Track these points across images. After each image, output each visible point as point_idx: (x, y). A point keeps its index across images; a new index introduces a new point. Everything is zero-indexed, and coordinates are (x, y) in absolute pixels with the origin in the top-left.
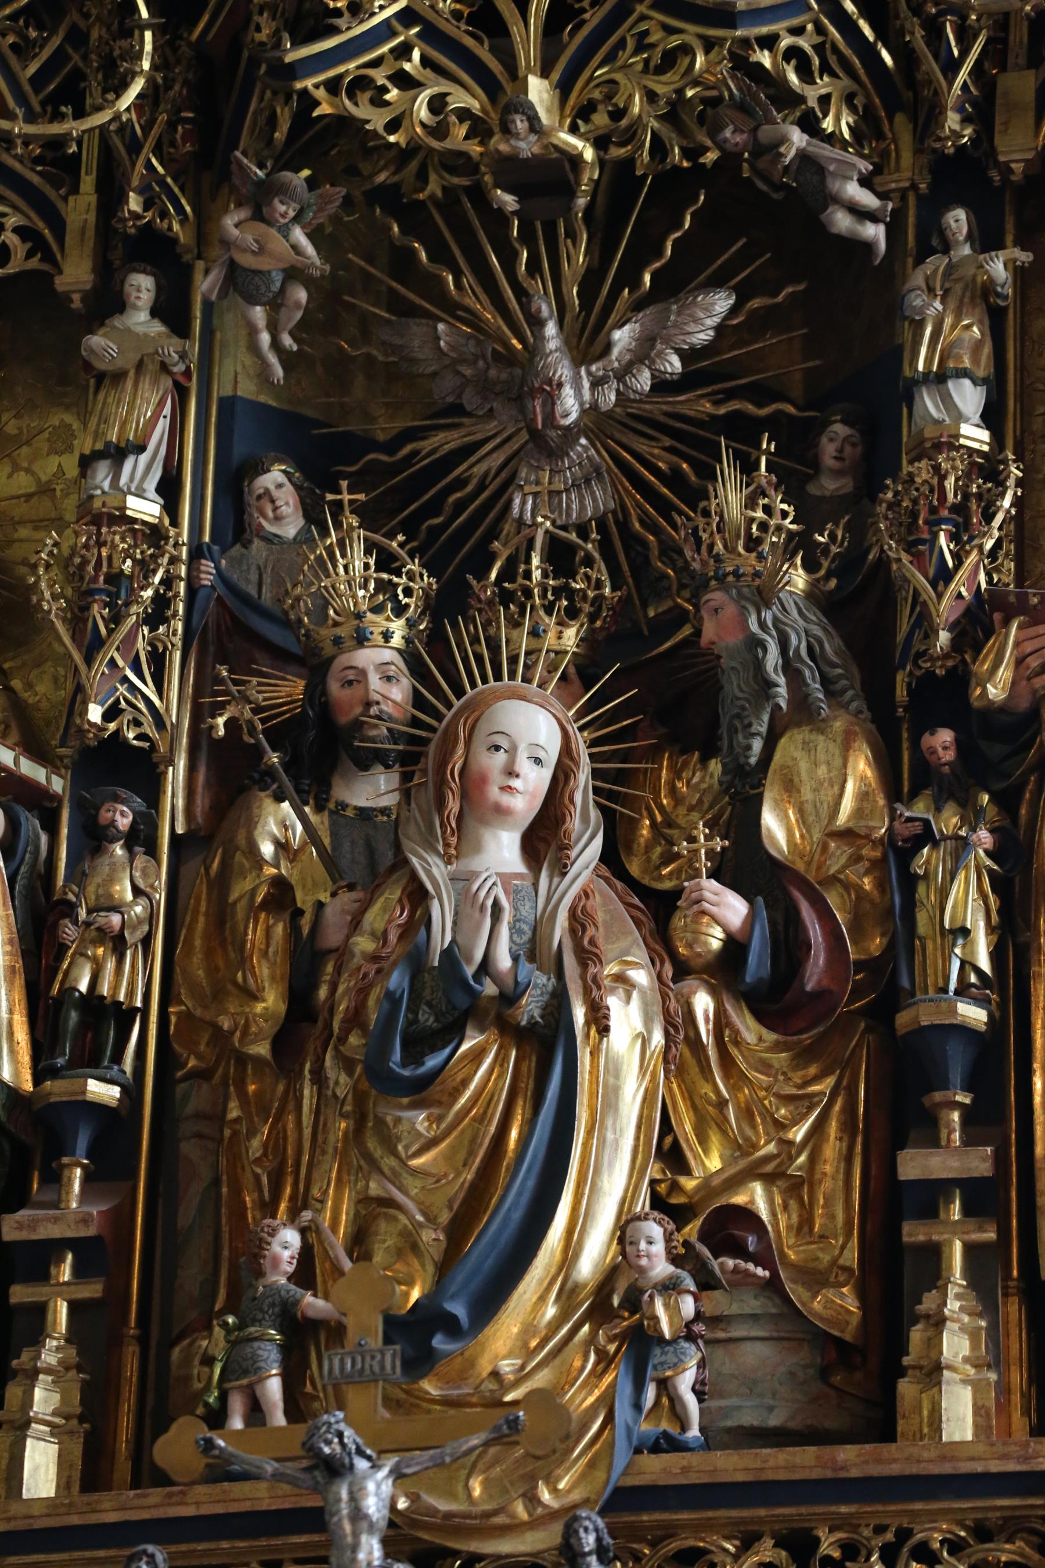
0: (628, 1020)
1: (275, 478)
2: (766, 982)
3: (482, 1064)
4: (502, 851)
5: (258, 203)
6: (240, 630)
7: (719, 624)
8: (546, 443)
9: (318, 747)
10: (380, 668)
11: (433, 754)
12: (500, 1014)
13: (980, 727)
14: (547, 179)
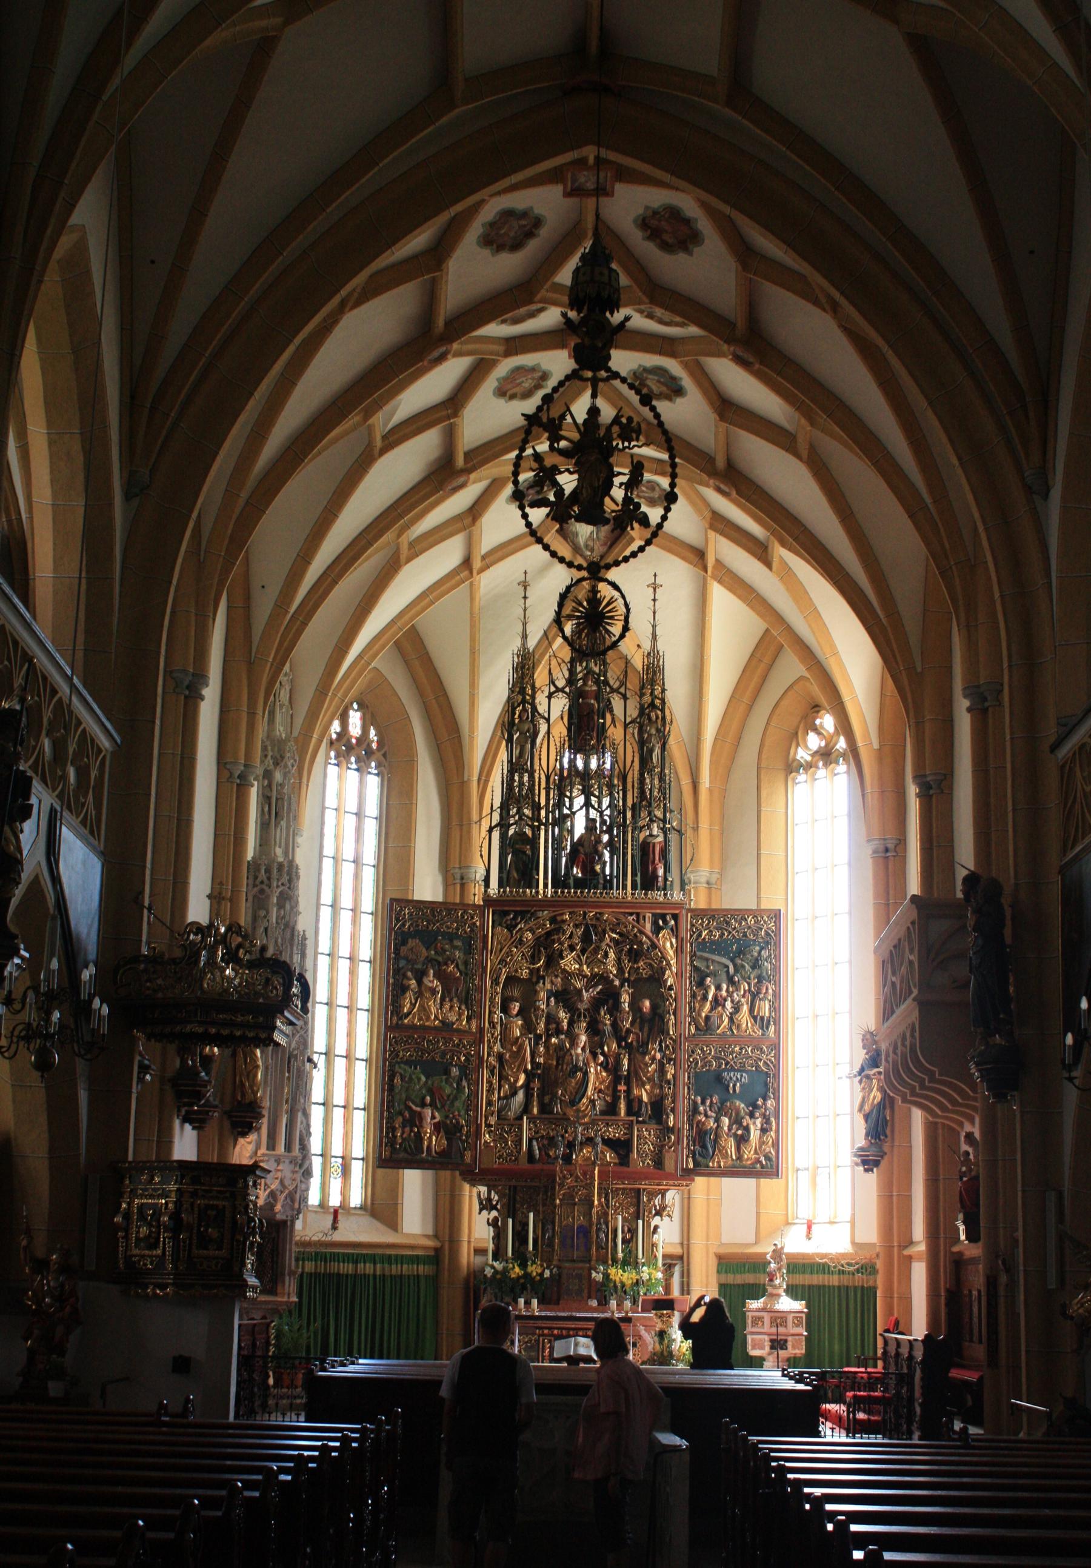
0: (592, 1070)
1: (552, 999)
2: (605, 1066)
4: (579, 1051)
5: (556, 976)
6: (551, 1019)
7: (600, 1026)
8: (582, 1001)
9: (558, 1032)
12: (581, 1069)
13: (627, 1043)
14: (585, 976)
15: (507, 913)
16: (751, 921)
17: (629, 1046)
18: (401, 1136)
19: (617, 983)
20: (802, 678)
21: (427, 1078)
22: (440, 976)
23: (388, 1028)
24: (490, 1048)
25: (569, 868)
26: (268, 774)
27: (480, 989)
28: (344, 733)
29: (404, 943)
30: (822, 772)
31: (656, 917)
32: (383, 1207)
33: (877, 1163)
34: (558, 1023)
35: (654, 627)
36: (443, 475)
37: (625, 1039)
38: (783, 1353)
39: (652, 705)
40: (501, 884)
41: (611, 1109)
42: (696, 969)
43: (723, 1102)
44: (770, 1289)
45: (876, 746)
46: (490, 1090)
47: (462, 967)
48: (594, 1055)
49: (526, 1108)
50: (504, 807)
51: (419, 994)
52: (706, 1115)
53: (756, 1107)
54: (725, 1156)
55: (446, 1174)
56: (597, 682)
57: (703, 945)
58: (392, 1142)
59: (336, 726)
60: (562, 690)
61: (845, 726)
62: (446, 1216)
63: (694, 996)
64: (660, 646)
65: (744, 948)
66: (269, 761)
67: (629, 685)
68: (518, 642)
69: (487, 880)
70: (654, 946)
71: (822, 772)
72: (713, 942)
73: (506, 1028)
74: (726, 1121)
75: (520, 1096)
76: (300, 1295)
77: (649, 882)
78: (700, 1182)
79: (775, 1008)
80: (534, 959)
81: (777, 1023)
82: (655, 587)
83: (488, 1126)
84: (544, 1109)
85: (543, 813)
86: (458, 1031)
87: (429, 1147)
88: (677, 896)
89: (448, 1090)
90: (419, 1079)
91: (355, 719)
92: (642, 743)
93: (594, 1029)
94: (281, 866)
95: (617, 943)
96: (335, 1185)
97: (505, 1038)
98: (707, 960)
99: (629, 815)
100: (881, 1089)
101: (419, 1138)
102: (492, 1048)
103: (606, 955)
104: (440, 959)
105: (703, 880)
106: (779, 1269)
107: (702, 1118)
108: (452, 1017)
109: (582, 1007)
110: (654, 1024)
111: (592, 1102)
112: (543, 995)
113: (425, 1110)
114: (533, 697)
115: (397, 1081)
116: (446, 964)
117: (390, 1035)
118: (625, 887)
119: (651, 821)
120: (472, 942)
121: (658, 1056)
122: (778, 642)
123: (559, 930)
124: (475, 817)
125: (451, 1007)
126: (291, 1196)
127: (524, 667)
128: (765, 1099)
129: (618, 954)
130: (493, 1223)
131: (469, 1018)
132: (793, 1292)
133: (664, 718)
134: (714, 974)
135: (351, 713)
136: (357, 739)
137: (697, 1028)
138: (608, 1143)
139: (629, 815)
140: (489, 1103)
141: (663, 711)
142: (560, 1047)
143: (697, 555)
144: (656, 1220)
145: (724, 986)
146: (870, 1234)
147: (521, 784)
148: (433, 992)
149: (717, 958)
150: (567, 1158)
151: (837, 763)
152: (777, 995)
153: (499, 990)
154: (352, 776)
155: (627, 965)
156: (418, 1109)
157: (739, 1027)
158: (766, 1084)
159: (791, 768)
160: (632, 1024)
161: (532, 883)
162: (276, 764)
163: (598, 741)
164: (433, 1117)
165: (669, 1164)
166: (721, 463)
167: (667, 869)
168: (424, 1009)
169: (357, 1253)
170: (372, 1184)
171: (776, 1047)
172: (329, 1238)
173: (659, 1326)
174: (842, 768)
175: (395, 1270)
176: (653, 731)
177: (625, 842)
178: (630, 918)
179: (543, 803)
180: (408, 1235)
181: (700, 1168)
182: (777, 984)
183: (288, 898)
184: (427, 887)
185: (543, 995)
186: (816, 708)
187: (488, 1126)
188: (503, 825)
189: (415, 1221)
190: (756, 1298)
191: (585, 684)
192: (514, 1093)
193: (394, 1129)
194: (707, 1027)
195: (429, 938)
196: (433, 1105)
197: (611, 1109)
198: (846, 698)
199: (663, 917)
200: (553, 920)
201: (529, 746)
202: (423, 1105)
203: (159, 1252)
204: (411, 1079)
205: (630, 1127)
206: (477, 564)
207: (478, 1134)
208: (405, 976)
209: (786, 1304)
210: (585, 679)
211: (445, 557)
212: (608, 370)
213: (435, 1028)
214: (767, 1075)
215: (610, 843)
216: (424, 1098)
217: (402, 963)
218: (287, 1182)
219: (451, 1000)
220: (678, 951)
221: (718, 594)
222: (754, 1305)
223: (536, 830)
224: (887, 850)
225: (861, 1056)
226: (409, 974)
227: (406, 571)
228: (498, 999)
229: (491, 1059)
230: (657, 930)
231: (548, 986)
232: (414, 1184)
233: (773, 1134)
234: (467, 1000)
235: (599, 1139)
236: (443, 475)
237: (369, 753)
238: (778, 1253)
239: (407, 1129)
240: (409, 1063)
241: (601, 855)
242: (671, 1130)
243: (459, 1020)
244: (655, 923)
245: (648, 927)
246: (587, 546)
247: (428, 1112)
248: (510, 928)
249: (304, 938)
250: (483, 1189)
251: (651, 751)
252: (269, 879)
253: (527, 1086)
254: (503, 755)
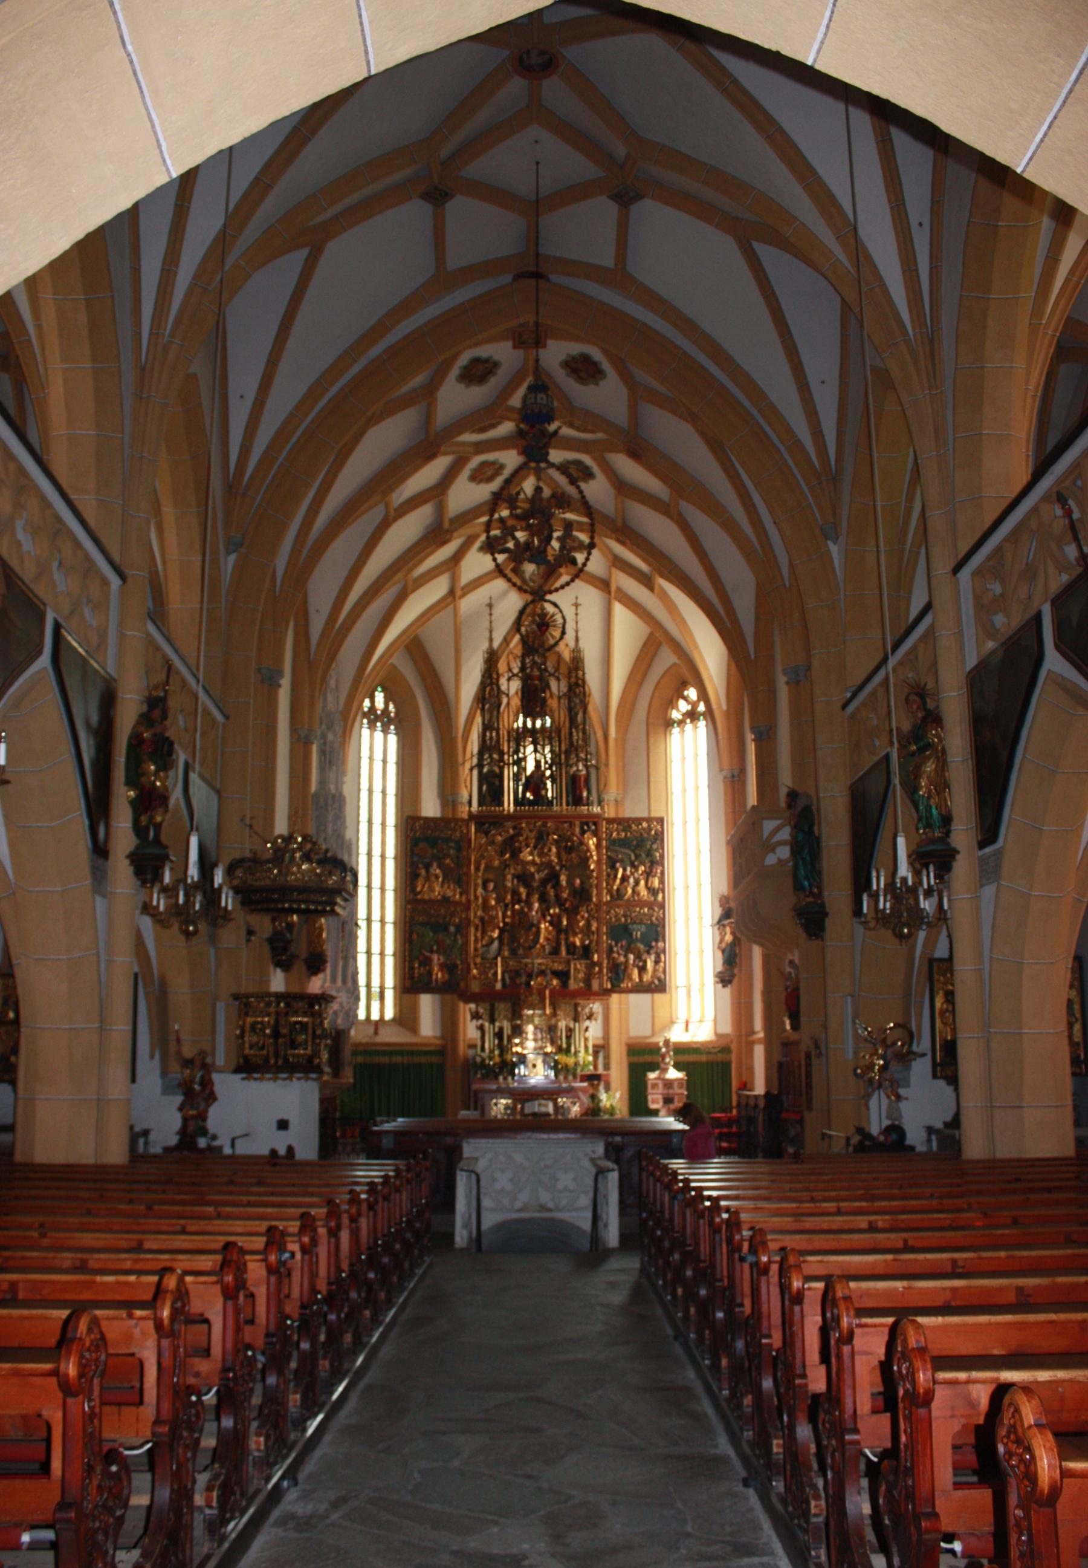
2: (551, 923)
3: (534, 929)
4: (534, 913)
6: (515, 893)
9: (519, 901)
10: (524, 896)
11: (530, 907)
15: (484, 824)
16: (645, 825)
17: (566, 910)
19: (558, 868)
20: (675, 664)
22: (439, 867)
23: (408, 902)
24: (475, 914)
25: (524, 793)
26: (324, 736)
27: (468, 874)
28: (372, 708)
30: (689, 726)
31: (582, 824)
32: (406, 1018)
33: (730, 982)
34: (519, 895)
35: (577, 632)
36: (436, 535)
37: (564, 905)
38: (672, 1106)
39: (577, 685)
40: (480, 804)
41: (555, 951)
42: (609, 857)
43: (629, 945)
44: (662, 1066)
45: (724, 707)
46: (476, 940)
48: (544, 916)
49: (499, 952)
50: (481, 754)
51: (427, 879)
52: (618, 953)
53: (651, 947)
54: (631, 979)
55: (448, 997)
56: (540, 669)
57: (612, 842)
58: (412, 978)
59: (367, 703)
60: (516, 675)
61: (703, 695)
62: (449, 1023)
63: (608, 875)
64: (581, 644)
65: (642, 844)
66: (324, 727)
67: (561, 671)
68: (486, 645)
69: (470, 803)
70: (581, 843)
71: (689, 726)
72: (620, 840)
73: (486, 901)
74: (631, 957)
75: (496, 944)
76: (355, 1077)
77: (577, 801)
78: (615, 997)
79: (662, 881)
80: (502, 854)
81: (663, 892)
82: (577, 605)
83: (475, 964)
84: (514, 952)
85: (506, 757)
88: (596, 810)
89: (448, 941)
91: (380, 698)
92: (570, 709)
93: (543, 899)
94: (334, 796)
95: (556, 842)
96: (375, 1005)
97: (486, 906)
98: (616, 851)
99: (563, 757)
100: (733, 933)
101: (430, 973)
102: (476, 913)
103: (550, 850)
105: (612, 799)
106: (668, 1052)
107: (615, 955)
108: (449, 893)
109: (535, 884)
110: (582, 895)
111: (543, 947)
112: (509, 877)
114: (498, 680)
115: (415, 936)
117: (409, 907)
118: (561, 805)
119: (578, 761)
120: (463, 843)
121: (586, 915)
122: (658, 640)
123: (519, 834)
124: (460, 760)
125: (449, 887)
126: (347, 1014)
127: (491, 660)
128: (657, 941)
129: (558, 848)
130: (481, 1028)
131: (461, 894)
132: (678, 1066)
133: (585, 692)
134: (621, 861)
135: (377, 693)
137: (612, 897)
138: (556, 974)
139: (563, 757)
140: (476, 949)
141: (584, 687)
142: (521, 911)
143: (604, 585)
144: (587, 1023)
145: (629, 869)
146: (727, 1028)
147: (491, 738)
148: (437, 877)
149: (623, 850)
150: (528, 984)
151: (698, 719)
152: (662, 873)
153: (480, 874)
154: (379, 735)
155: (564, 856)
157: (638, 894)
158: (657, 933)
159: (669, 724)
160: (569, 894)
161: (501, 803)
162: (329, 728)
163: (542, 708)
165: (595, 985)
166: (619, 523)
167: (589, 792)
168: (431, 889)
169: (391, 1050)
170: (399, 1004)
171: (662, 906)
172: (372, 1041)
173: (591, 1091)
174: (702, 724)
175: (416, 1060)
176: (578, 701)
177: (561, 775)
178: (566, 825)
179: (506, 750)
180: (426, 1037)
181: (616, 988)
182: (663, 866)
183: (340, 817)
184: (430, 807)
185: (509, 877)
186: (684, 685)
187: (475, 964)
188: (480, 766)
189: (428, 1026)
190: (653, 1070)
191: (532, 670)
192: (492, 940)
193: (412, 968)
194: (619, 895)
195: (433, 842)
196: (438, 952)
197: (555, 951)
198: (705, 676)
199: (587, 824)
200: (514, 828)
201: (495, 713)
202: (432, 951)
203: (265, 1052)
205: (568, 963)
206: (458, 592)
207: (469, 970)
208: (417, 867)
209: (673, 1074)
210: (532, 667)
211: (437, 589)
212: (547, 462)
213: (438, 901)
214: (658, 926)
215: (551, 776)
216: (432, 947)
218: (345, 1005)
220: (598, 846)
221: (619, 609)
222: (652, 1076)
223: (502, 769)
224: (733, 776)
225: (719, 911)
226: (420, 866)
227: (412, 598)
228: (480, 881)
229: (477, 921)
230: (583, 832)
231: (512, 871)
232: (427, 1003)
233: (662, 964)
234: (459, 882)
235: (548, 971)
236: (436, 535)
237: (390, 721)
238: (667, 1042)
240: (422, 924)
241: (545, 784)
242: (594, 964)
243: (454, 895)
244: (582, 829)
245: (577, 830)
246: (531, 580)
247: (435, 957)
248: (486, 833)
249: (350, 844)
250: (473, 1006)
251: (577, 714)
252: (326, 805)
253: (500, 937)
254: (478, 720)
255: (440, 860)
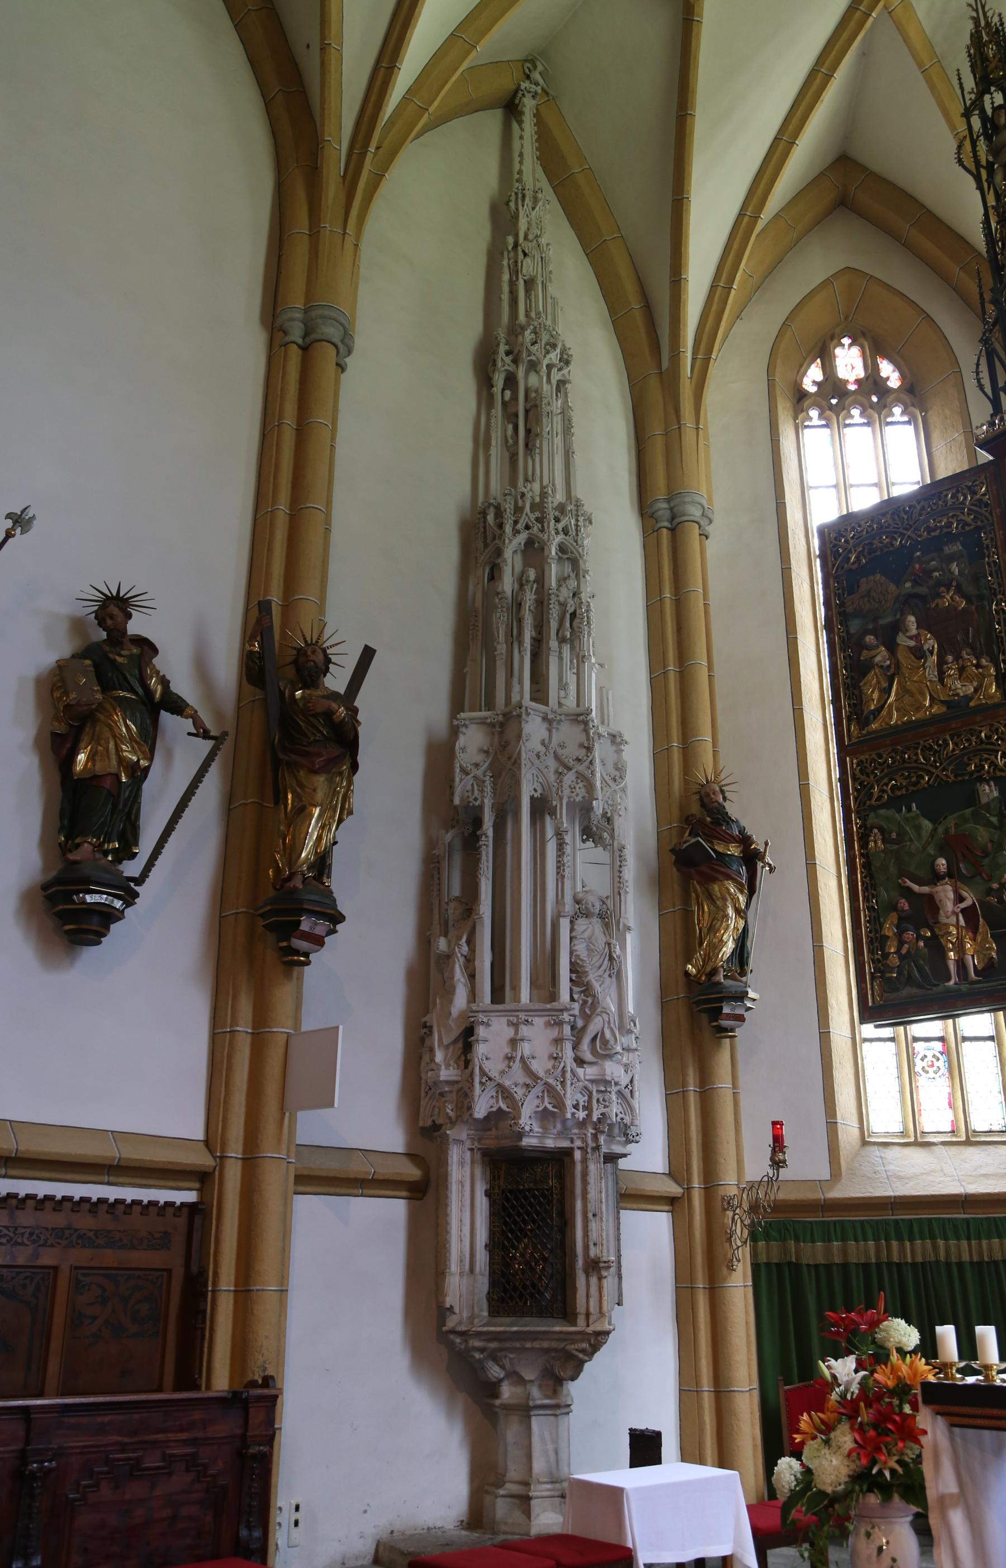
18: (898, 952)
21: (934, 821)
29: (852, 588)
47: (971, 590)
86: (981, 709)
87: (961, 964)
89: (983, 835)
90: (918, 828)
104: (923, 590)
113: (939, 888)
116: (939, 596)
125: (961, 670)
135: (838, 351)
136: (858, 381)
156: (925, 889)
164: (960, 899)
202: (936, 878)
204: (902, 834)
213: (934, 720)
216: (933, 864)
217: (855, 626)
219: (958, 657)
239: (910, 935)
240: (895, 803)
247: (945, 893)
255: (917, 602)
